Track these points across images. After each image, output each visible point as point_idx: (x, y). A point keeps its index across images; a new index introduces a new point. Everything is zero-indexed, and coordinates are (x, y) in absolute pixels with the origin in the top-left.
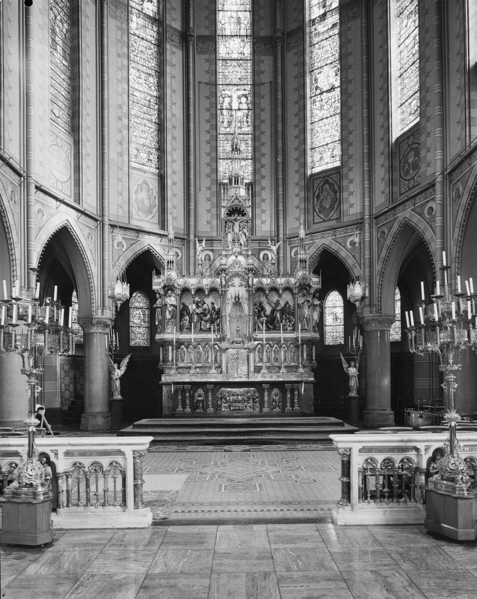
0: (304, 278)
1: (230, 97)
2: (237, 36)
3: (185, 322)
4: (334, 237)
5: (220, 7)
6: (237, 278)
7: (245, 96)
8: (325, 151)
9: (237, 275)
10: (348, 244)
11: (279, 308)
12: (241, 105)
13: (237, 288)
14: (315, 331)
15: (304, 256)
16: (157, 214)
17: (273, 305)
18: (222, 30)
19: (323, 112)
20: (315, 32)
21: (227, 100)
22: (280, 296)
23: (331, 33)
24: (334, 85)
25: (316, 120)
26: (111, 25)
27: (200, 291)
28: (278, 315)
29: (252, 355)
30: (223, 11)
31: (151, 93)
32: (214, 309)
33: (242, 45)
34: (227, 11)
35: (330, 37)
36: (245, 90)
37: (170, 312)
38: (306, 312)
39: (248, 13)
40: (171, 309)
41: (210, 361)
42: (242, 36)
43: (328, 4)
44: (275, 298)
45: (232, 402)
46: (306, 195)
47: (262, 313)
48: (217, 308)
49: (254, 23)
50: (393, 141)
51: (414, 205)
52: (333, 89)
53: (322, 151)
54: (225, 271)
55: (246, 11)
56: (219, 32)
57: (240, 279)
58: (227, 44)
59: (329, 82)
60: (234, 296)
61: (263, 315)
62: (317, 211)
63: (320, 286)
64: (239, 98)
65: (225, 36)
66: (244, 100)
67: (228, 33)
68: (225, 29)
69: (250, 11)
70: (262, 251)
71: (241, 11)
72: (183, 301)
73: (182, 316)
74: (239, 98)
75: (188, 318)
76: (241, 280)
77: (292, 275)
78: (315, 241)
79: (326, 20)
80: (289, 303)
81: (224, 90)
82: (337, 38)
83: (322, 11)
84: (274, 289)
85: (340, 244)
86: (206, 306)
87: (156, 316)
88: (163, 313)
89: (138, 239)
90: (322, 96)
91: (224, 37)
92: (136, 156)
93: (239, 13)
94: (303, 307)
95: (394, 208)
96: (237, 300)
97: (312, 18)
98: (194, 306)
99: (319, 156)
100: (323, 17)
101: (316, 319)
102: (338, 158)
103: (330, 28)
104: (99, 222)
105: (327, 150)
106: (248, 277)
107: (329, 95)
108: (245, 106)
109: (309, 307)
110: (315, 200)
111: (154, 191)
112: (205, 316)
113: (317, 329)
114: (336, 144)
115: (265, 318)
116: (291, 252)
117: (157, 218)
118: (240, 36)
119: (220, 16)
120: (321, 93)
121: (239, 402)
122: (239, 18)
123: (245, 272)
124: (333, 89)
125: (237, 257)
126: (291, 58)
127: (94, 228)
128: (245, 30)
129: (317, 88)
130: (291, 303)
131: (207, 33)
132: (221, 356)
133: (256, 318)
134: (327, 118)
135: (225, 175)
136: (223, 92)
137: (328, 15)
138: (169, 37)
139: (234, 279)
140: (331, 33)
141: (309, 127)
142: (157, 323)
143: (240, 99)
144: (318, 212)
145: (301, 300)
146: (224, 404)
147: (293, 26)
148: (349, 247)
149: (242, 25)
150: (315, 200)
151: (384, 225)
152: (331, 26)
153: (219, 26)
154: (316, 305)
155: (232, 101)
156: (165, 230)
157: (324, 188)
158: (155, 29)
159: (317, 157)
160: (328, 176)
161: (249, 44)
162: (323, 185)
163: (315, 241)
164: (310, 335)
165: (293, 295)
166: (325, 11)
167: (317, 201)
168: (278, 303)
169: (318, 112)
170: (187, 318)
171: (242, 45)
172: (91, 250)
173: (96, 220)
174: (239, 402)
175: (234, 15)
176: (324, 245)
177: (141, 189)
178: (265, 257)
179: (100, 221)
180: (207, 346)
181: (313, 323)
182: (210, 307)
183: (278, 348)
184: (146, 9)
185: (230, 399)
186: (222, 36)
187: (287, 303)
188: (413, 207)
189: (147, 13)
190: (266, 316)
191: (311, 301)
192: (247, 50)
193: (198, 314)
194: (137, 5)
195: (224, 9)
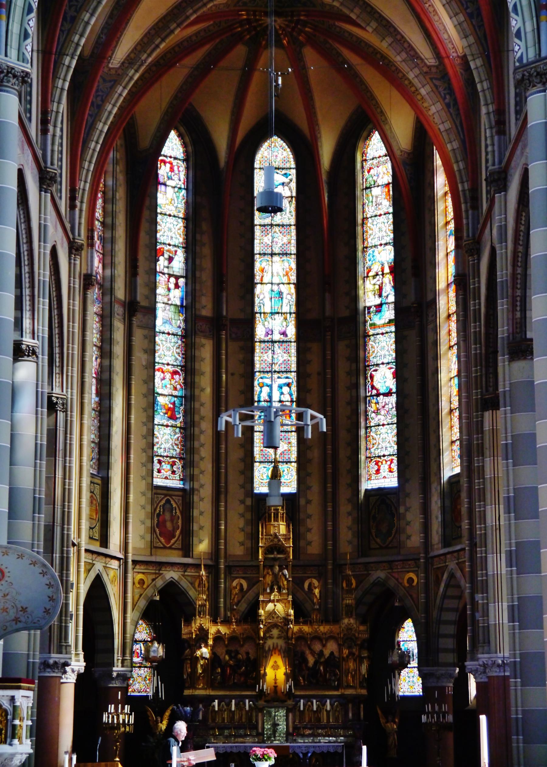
0: (349, 628)
1: (270, 386)
2: (278, 313)
3: (217, 675)
4: (390, 571)
5: (257, 279)
6: (275, 629)
7: (289, 385)
8: (382, 463)
9: (275, 626)
10: (405, 581)
11: (322, 660)
12: (282, 396)
13: (275, 641)
14: (362, 687)
15: (350, 601)
16: (180, 537)
17: (316, 656)
18: (260, 307)
19: (379, 417)
20: (371, 322)
21: (266, 390)
22: (324, 646)
23: (387, 329)
24: (391, 390)
25: (372, 424)
26: (138, 335)
27: (233, 638)
28: (321, 668)
29: (290, 715)
30: (261, 284)
31: (175, 393)
32: (248, 658)
33: (284, 324)
34: (266, 284)
35: (387, 333)
36: (287, 378)
37: (201, 665)
38: (351, 665)
39: (292, 286)
40: (202, 662)
41: (244, 720)
42: (284, 313)
43: (384, 294)
44: (317, 647)
47: (304, 665)
48: (252, 658)
49: (299, 303)
50: (445, 480)
51: (458, 559)
52: (389, 394)
53: (379, 461)
54: (262, 622)
55: (289, 284)
56: (257, 309)
58: (266, 323)
59: (387, 384)
61: (304, 668)
63: (366, 636)
64: (280, 387)
65: (264, 313)
66: (286, 389)
67: (267, 309)
68: (264, 305)
69: (294, 284)
70: (306, 580)
71: (283, 284)
72: (214, 650)
73: (214, 668)
74: (280, 387)
75: (220, 671)
77: (336, 620)
78: (370, 572)
79: (383, 313)
80: (335, 653)
81: (262, 378)
82: (393, 335)
83: (378, 301)
84: (317, 637)
86: (241, 656)
87: (185, 670)
88: (194, 668)
89: (161, 572)
90: (378, 398)
91: (262, 314)
92: (159, 471)
93: (281, 286)
94: (347, 661)
95: (445, 554)
97: (368, 304)
98: (227, 657)
99: (376, 467)
100: (379, 308)
101: (363, 673)
102: (396, 474)
103: (386, 322)
104: (122, 561)
105: (384, 462)
106: (288, 629)
107: (387, 399)
108: (287, 398)
109: (355, 660)
111: (178, 511)
112: (241, 668)
113: (365, 685)
114: (393, 457)
115: (307, 672)
117: (180, 542)
118: (282, 313)
119: (258, 289)
120: (378, 395)
122: (280, 293)
123: (283, 622)
124: (389, 394)
125: (275, 605)
126: (342, 347)
127: (117, 568)
128: (288, 305)
129: (373, 387)
130: (336, 654)
131: (242, 316)
132: (257, 716)
133: (297, 671)
134: (383, 425)
135: (262, 481)
136: (261, 380)
137: (384, 307)
138: (198, 329)
140: (387, 329)
141: (362, 432)
142: (185, 677)
143: (281, 388)
144: (374, 536)
145: (346, 652)
147: (345, 313)
148: (407, 585)
149: (284, 300)
151: (438, 568)
152: (387, 321)
153: (257, 301)
154: (364, 657)
155: (271, 389)
156: (189, 557)
158: (182, 318)
159: (373, 467)
161: (293, 322)
163: (370, 572)
164: (355, 693)
165: (340, 646)
166: (381, 301)
168: (321, 653)
169: (373, 415)
170: (219, 670)
171: (284, 324)
172: (114, 594)
173: (119, 559)
175: (275, 288)
176: (379, 579)
179: (123, 559)
180: (241, 703)
181: (359, 677)
182: (245, 657)
183: (321, 707)
184: (172, 299)
186: (260, 313)
187: (332, 653)
188: (457, 561)
189: (173, 303)
190: (308, 668)
191: (357, 653)
192: (291, 332)
193: (230, 666)
194: (163, 297)
195: (264, 281)
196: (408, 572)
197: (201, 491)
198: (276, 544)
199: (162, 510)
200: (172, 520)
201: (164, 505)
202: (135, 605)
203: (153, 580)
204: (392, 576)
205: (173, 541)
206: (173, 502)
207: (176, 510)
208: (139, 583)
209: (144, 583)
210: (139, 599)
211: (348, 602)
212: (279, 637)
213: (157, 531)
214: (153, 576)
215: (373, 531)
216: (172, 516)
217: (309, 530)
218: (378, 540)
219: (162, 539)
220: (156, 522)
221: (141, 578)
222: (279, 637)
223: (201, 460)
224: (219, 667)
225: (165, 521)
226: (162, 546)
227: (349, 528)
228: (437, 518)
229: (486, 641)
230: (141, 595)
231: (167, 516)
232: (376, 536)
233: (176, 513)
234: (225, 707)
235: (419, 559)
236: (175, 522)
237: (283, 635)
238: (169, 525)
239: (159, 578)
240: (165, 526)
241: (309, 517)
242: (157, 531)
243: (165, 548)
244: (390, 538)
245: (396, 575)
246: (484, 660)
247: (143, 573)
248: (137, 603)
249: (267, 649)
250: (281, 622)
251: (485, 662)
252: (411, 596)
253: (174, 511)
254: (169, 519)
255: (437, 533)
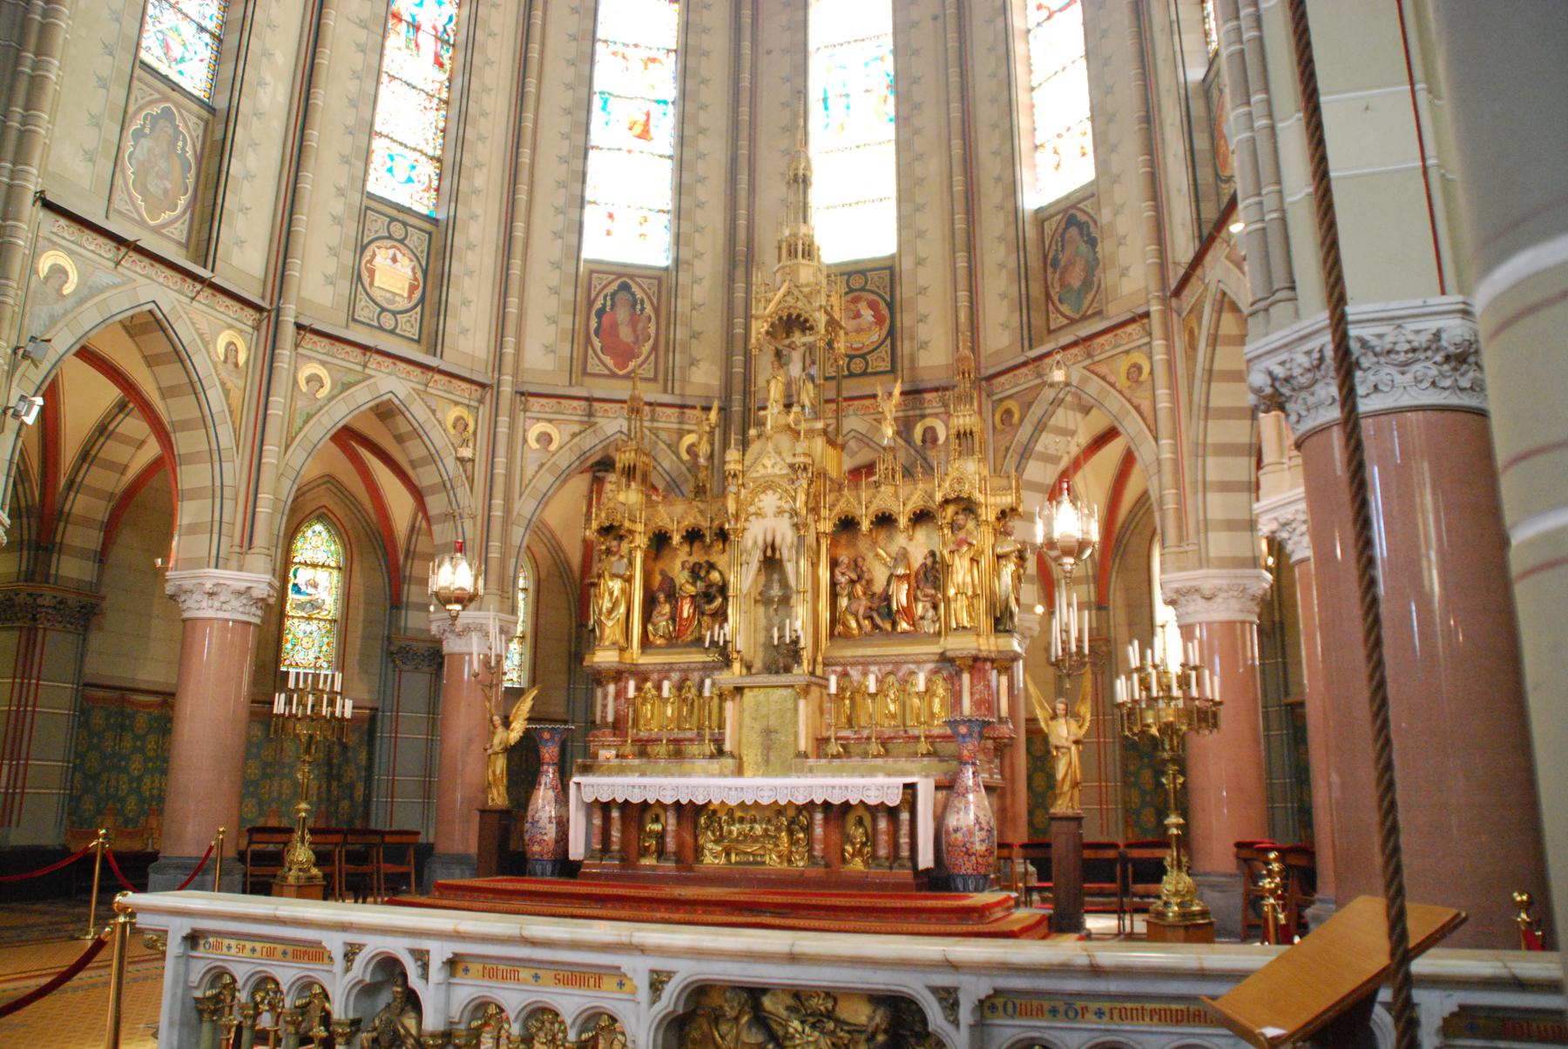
4: (1088, 362)
6: (770, 492)
15: (967, 419)
45: (737, 840)
46: (1022, 261)
57: (778, 495)
60: (760, 542)
62: (1056, 299)
76: (781, 498)
85: (1104, 378)
96: (769, 553)
110: (1050, 270)
111: (647, 305)
116: (993, 415)
121: (756, 839)
139: (762, 496)
146: (710, 845)
150: (1050, 270)
157: (1067, 237)
160: (1074, 206)
162: (1065, 230)
167: (1054, 273)
174: (756, 839)
177: (613, 305)
178: (928, 436)
185: (730, 832)
196: (1127, 352)
197: (697, 262)
198: (789, 308)
199: (609, 303)
200: (633, 322)
201: (613, 295)
202: (527, 486)
203: (574, 435)
204: (1092, 372)
205: (632, 365)
206: (635, 288)
207: (642, 302)
208: (538, 440)
209: (551, 441)
210: (537, 472)
211: (961, 421)
212: (780, 512)
213: (597, 343)
214: (577, 428)
215: (1055, 292)
216: (633, 314)
217: (922, 319)
218: (1064, 308)
219: (608, 360)
220: (594, 323)
221: (543, 429)
222: (780, 512)
223: (698, 206)
224: (666, 601)
225: (614, 325)
226: (606, 372)
227: (1003, 296)
228: (1179, 190)
229: (1279, 281)
230: (541, 466)
231: (622, 315)
232: (1061, 301)
233: (643, 310)
234: (654, 692)
235: (1147, 315)
236: (640, 326)
237: (787, 507)
238: (625, 334)
239: (588, 432)
240: (617, 336)
241: (922, 291)
242: (597, 343)
243: (613, 375)
244: (1090, 297)
245: (1103, 369)
246: (1272, 364)
247: (550, 421)
248: (530, 481)
249: (750, 543)
250: (781, 476)
251: (1280, 372)
252: (1137, 408)
253: (639, 307)
254: (627, 319)
255: (1183, 225)
